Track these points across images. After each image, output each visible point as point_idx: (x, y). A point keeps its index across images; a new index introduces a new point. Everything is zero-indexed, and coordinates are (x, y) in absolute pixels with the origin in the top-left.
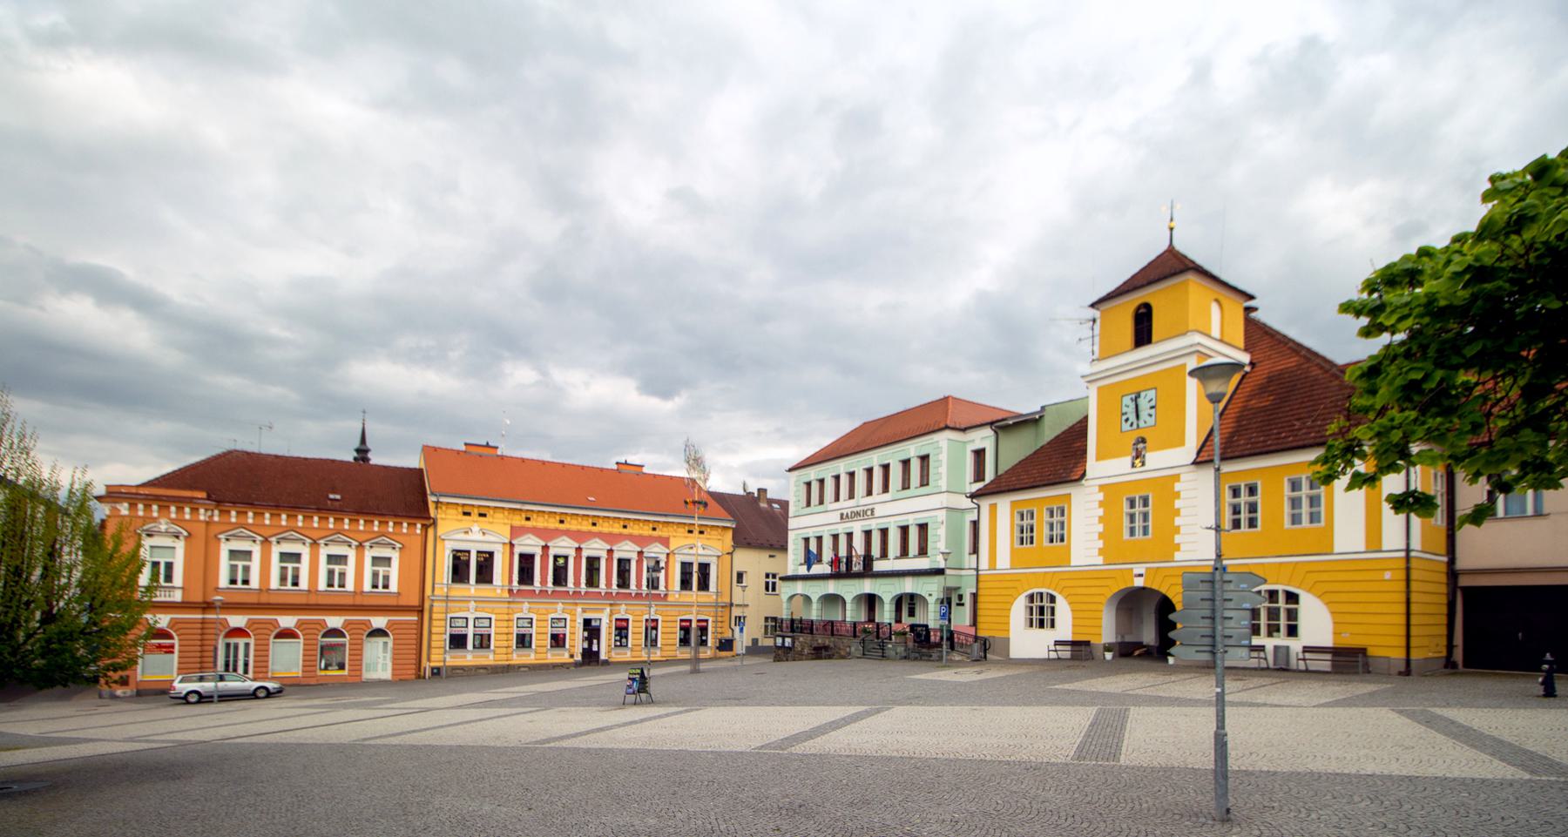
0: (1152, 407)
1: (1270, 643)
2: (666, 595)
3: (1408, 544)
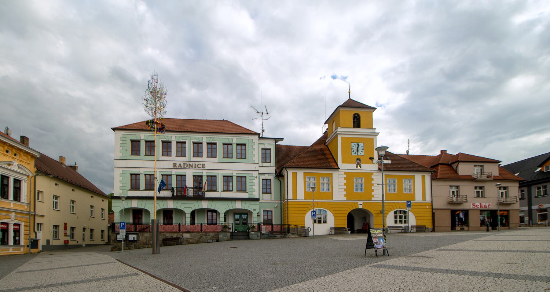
0: (362, 149)
3: (432, 200)
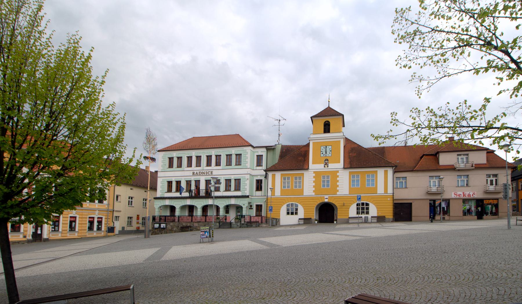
0: (330, 151)
1: (363, 216)
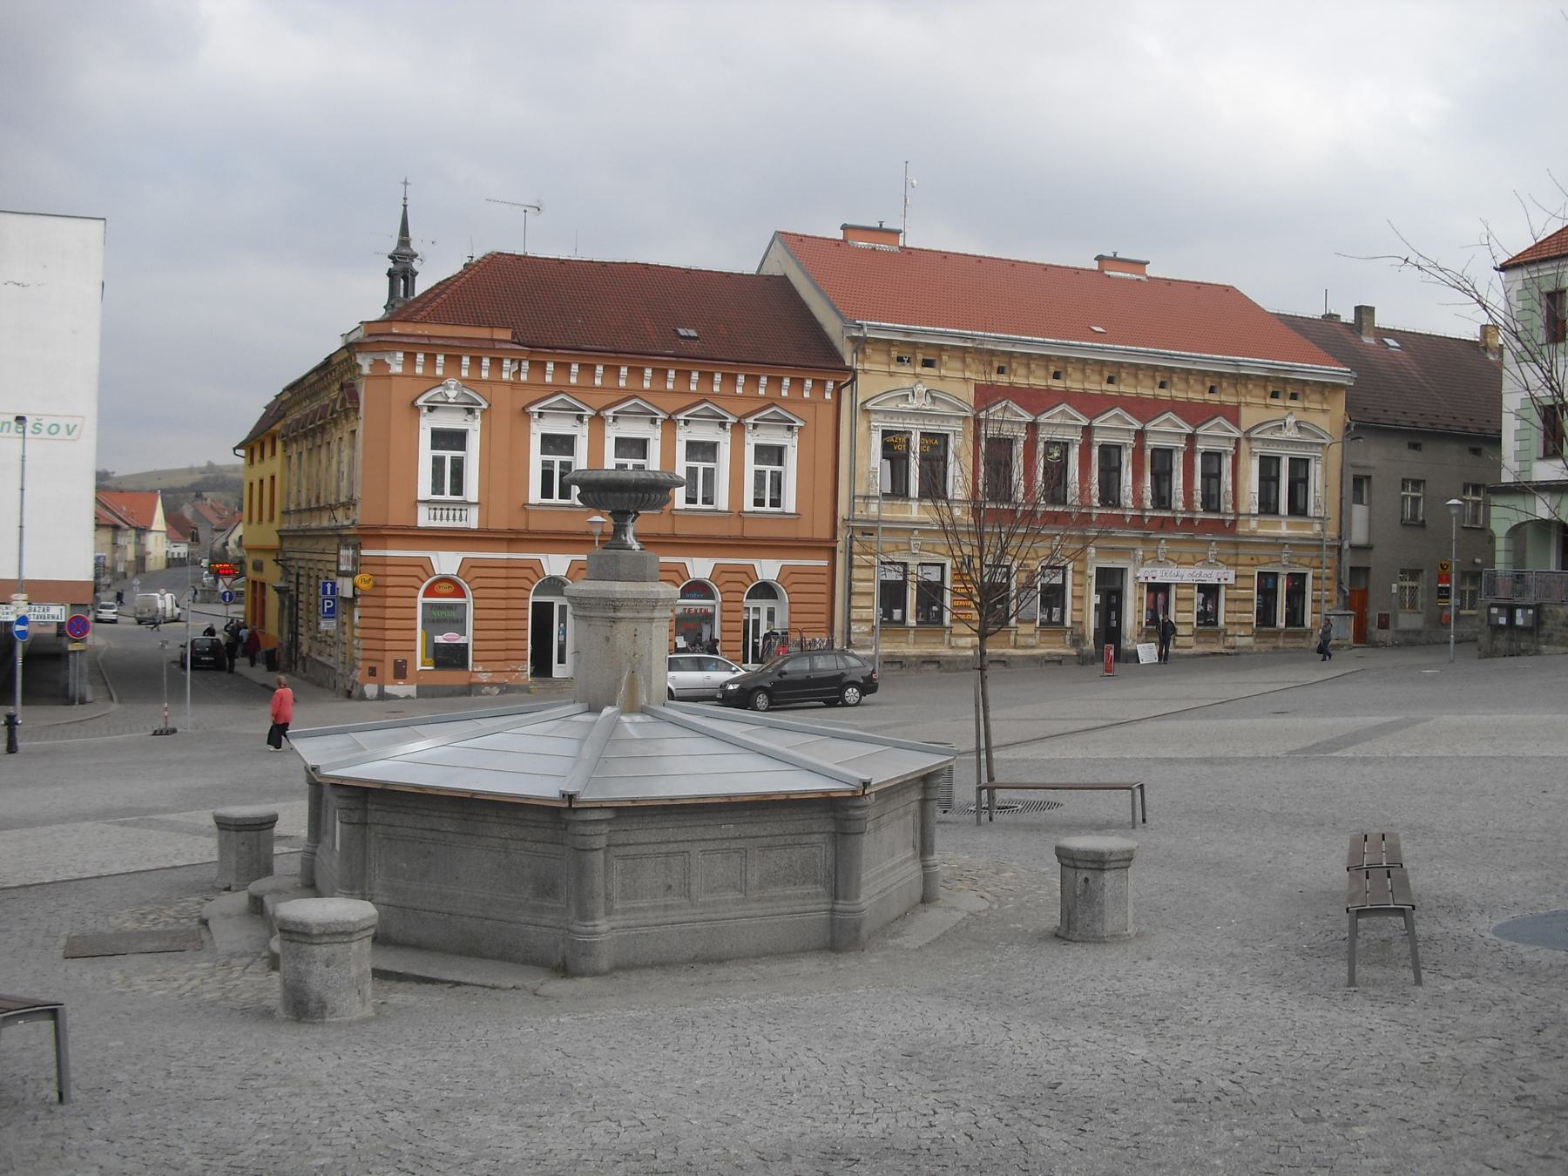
2: (1234, 523)
